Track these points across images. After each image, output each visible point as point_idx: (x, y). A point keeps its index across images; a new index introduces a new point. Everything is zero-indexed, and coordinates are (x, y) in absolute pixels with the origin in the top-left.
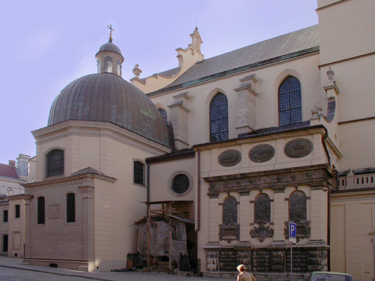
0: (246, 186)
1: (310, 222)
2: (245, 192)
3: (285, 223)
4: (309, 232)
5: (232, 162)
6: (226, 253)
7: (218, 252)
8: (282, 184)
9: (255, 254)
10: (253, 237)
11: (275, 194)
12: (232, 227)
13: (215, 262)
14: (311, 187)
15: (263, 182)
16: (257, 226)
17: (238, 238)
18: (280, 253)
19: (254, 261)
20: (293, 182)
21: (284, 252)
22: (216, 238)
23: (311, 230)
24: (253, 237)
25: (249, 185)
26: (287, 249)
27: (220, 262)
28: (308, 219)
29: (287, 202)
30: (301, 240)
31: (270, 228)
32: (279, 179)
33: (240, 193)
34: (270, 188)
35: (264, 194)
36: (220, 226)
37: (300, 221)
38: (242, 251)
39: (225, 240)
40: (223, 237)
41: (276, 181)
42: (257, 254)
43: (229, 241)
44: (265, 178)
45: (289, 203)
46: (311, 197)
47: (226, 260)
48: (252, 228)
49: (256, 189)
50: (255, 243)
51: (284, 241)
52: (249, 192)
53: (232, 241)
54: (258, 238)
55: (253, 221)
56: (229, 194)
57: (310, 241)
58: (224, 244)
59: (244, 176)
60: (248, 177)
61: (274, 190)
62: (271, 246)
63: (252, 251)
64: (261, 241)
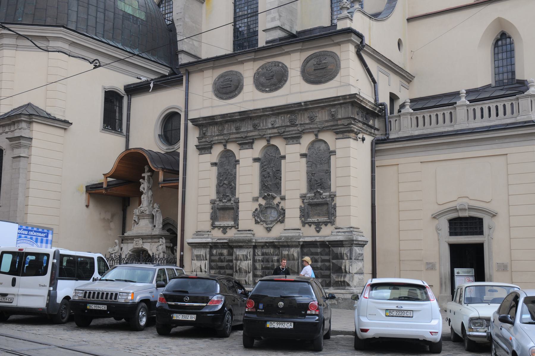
0: (247, 132)
1: (335, 196)
2: (247, 143)
3: (301, 197)
4: (334, 215)
5: (231, 92)
6: (219, 251)
7: (208, 250)
8: (296, 128)
9: (260, 253)
10: (257, 222)
11: (288, 147)
12: (229, 204)
13: (203, 268)
14: (337, 133)
15: (270, 126)
16: (262, 202)
17: (236, 226)
18: (292, 250)
19: (258, 265)
20: (311, 126)
21: (299, 249)
22: (207, 226)
23: (337, 209)
24: (257, 222)
25: (251, 131)
26: (301, 243)
27: (211, 268)
28: (333, 189)
29: (304, 160)
30: (323, 227)
31: (280, 205)
32: (293, 119)
33: (240, 144)
34: (280, 135)
35: (273, 145)
36: (213, 202)
37: (321, 194)
38: (241, 247)
39: (219, 227)
40: (217, 223)
41: (289, 124)
42: (263, 254)
43: (224, 229)
44: (272, 119)
45: (307, 162)
46: (337, 151)
47: (220, 264)
48: (256, 206)
49: (262, 137)
50: (260, 234)
51: (300, 229)
52: (252, 143)
53: (228, 230)
54: (265, 225)
55: (256, 194)
56: (225, 146)
57: (336, 228)
58: (217, 235)
60: (251, 118)
61: (285, 138)
62: (280, 238)
63: (255, 247)
64: (269, 230)
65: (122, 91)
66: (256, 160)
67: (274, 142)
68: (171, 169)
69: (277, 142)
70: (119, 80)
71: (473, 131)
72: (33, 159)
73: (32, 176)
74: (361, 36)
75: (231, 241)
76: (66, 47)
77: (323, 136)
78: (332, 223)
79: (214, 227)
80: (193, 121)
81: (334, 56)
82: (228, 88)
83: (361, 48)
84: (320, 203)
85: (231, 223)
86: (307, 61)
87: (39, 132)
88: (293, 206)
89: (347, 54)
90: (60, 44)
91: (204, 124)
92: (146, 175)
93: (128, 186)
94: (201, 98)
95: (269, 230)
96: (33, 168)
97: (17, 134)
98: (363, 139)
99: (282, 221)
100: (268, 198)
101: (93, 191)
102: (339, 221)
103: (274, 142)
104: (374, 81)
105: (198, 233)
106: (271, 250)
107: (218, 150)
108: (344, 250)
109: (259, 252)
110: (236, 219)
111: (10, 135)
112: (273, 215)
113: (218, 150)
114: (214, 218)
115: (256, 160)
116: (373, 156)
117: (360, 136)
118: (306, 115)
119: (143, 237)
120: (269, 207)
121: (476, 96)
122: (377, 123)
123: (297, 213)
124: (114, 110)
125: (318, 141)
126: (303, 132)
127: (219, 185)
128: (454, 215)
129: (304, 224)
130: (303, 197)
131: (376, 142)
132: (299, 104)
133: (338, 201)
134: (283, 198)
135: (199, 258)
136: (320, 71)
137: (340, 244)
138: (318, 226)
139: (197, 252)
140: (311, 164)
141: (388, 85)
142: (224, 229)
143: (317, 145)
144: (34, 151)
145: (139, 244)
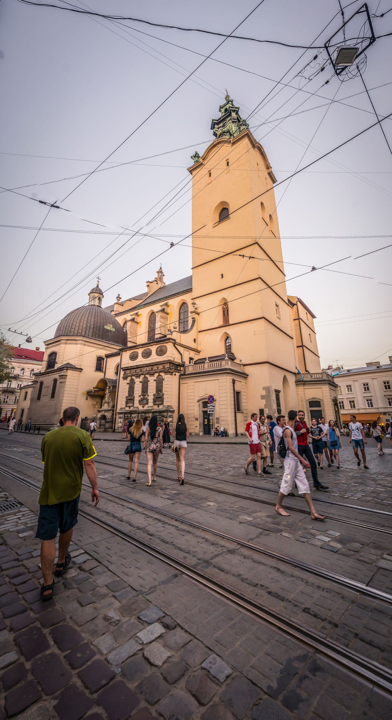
2: (138, 376)
16: (142, 397)
17: (133, 406)
22: (124, 406)
29: (155, 382)
36: (127, 397)
43: (130, 407)
44: (146, 368)
49: (143, 374)
50: (141, 408)
55: (140, 394)
59: (138, 367)
64: (143, 407)
65: (104, 357)
66: (140, 382)
67: (146, 376)
68: (115, 385)
69: (147, 376)
70: (103, 353)
71: (209, 372)
72: (67, 383)
73: (66, 389)
74: (174, 340)
75: (131, 411)
76: (83, 342)
77: (161, 374)
78: (163, 404)
79: (126, 406)
80: (122, 368)
81: (165, 347)
82: (134, 357)
83: (175, 343)
84: (159, 398)
85: (132, 405)
86: (158, 348)
87: (70, 373)
88: (151, 398)
89: (169, 346)
90: (80, 342)
91: (125, 369)
92: (108, 387)
93: (101, 392)
94: (126, 360)
95: (143, 407)
96: (66, 386)
97: (63, 374)
98: (175, 375)
99: (147, 404)
100: (144, 395)
101: (90, 394)
102: (165, 404)
103: (146, 376)
104: (181, 354)
105: (121, 409)
106: (143, 415)
107: (129, 378)
108: (165, 414)
109: (140, 415)
110: (133, 404)
111: (60, 374)
112: (145, 401)
113: (129, 378)
114: (127, 403)
115: (140, 382)
116: (179, 380)
117: (174, 373)
118: (156, 366)
119: (105, 411)
120: (144, 399)
121: (212, 359)
122: (182, 369)
123: (152, 401)
124: (100, 366)
125: (159, 375)
126: (155, 372)
127: (129, 391)
128: (204, 401)
129: (154, 405)
130: (154, 395)
131: (181, 375)
132: (153, 363)
133: (165, 397)
134: (148, 396)
135: (120, 418)
136: (161, 352)
137: (164, 412)
138: (158, 405)
139: (120, 416)
140: (157, 384)
141: (187, 355)
142: (130, 407)
143: (160, 377)
144: (67, 380)
145: (103, 413)
